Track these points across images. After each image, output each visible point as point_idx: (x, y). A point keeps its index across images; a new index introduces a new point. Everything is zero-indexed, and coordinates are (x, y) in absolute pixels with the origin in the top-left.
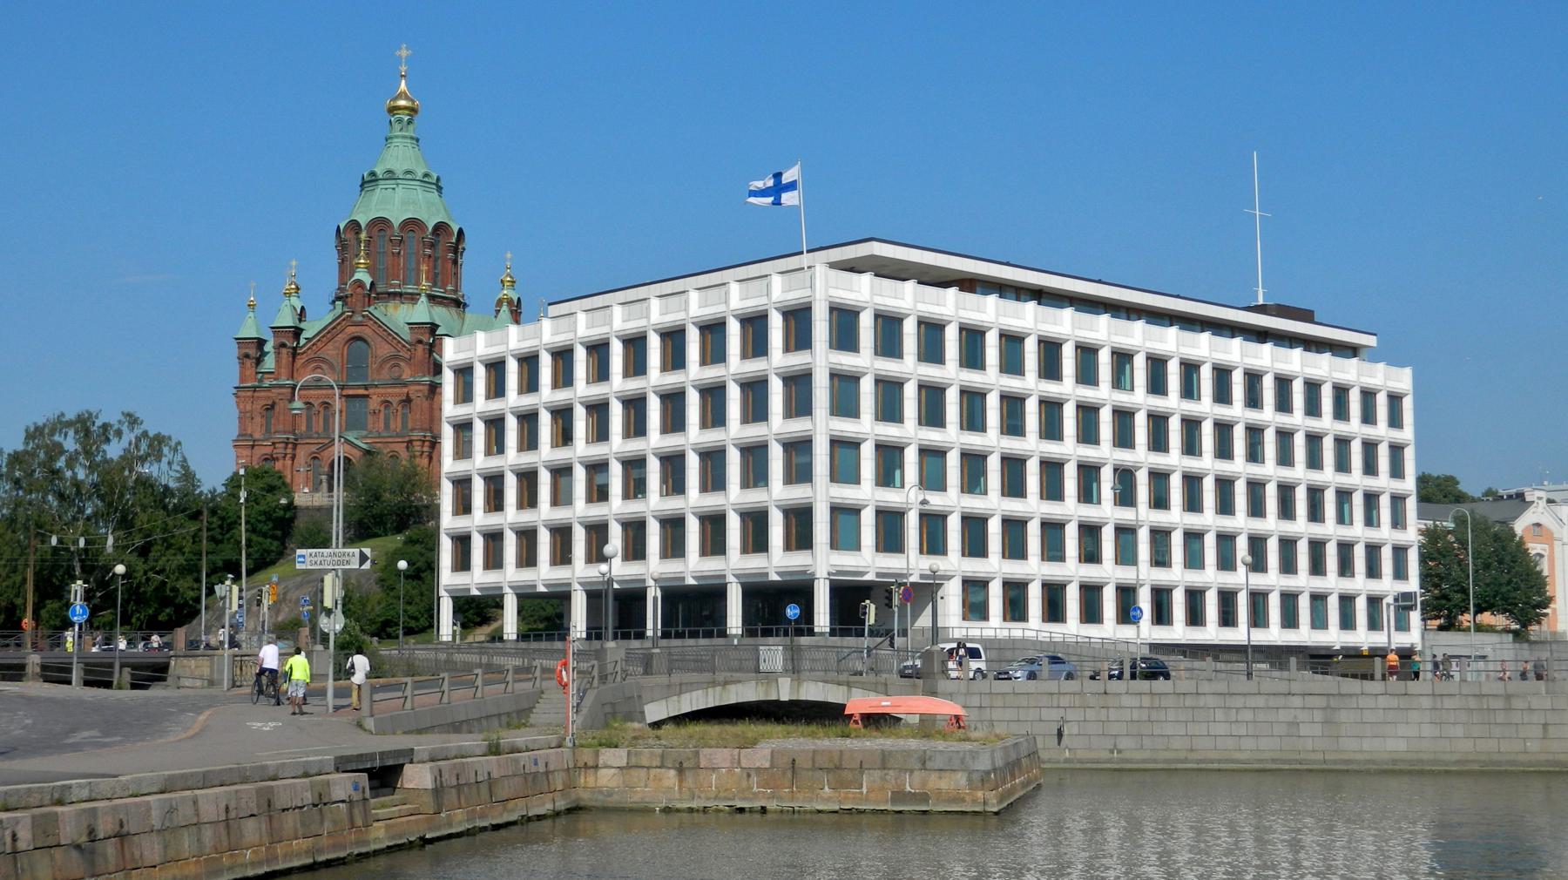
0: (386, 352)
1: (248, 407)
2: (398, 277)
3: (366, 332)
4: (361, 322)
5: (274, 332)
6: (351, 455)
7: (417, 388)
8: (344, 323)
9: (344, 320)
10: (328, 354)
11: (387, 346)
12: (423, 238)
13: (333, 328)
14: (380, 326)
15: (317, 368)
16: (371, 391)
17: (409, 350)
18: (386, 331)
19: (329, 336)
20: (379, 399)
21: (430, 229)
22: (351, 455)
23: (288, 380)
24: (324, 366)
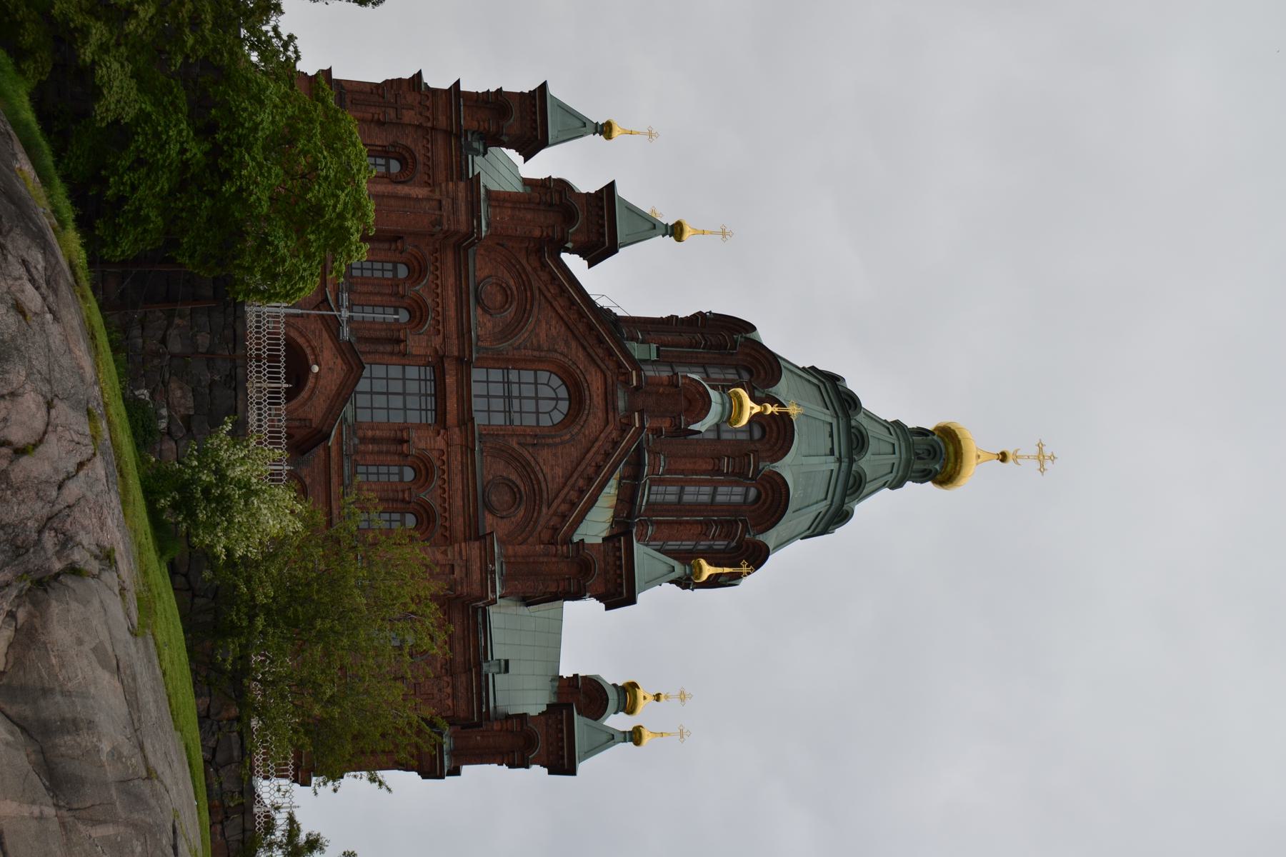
0: (544, 468)
1: (409, 116)
2: (668, 471)
3: (594, 422)
4: (615, 409)
6: (313, 391)
7: (476, 567)
8: (612, 365)
9: (620, 365)
10: (538, 320)
11: (559, 471)
12: (744, 523)
14: (608, 455)
15: (505, 290)
16: (456, 434)
17: (555, 530)
18: (597, 473)
20: (434, 456)
21: (761, 538)
22: (310, 398)
23: (488, 225)
24: (510, 312)
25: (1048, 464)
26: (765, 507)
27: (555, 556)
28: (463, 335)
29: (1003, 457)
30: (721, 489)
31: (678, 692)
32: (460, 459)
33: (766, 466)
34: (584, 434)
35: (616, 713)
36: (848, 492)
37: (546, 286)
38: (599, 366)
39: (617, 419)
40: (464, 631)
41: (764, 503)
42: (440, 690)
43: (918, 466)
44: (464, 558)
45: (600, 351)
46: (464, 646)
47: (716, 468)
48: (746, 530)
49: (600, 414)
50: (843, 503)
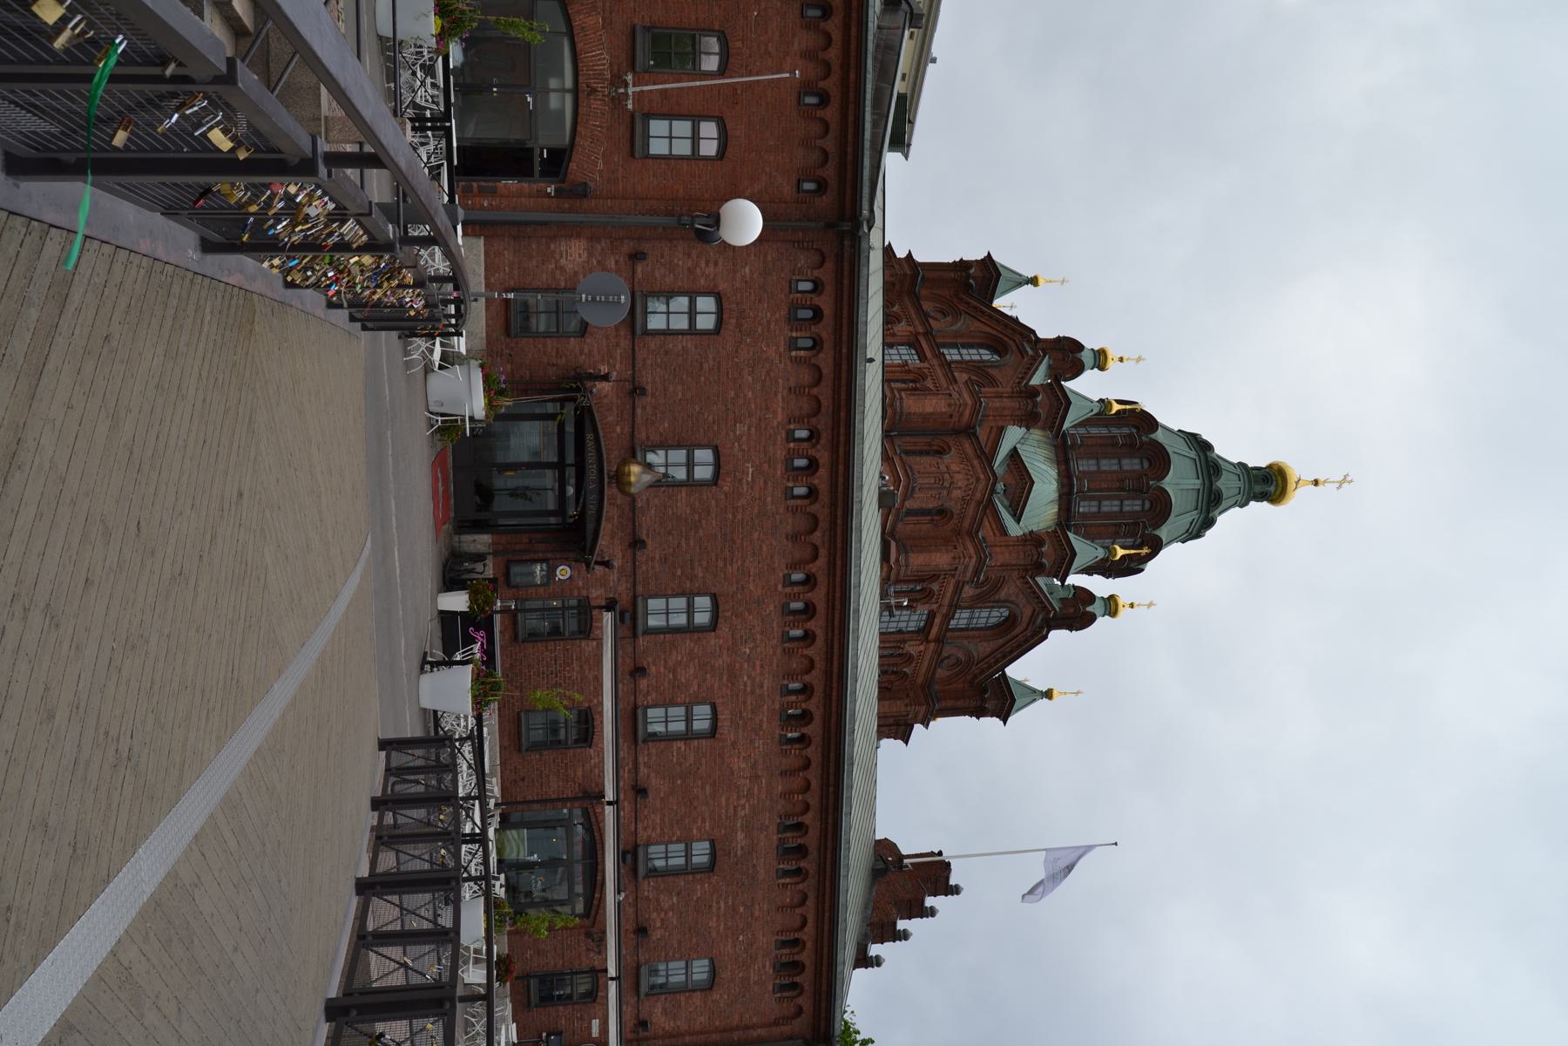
16: (935, 362)
29: (1316, 483)
35: (1103, 616)
43: (1258, 488)
50: (1211, 484)
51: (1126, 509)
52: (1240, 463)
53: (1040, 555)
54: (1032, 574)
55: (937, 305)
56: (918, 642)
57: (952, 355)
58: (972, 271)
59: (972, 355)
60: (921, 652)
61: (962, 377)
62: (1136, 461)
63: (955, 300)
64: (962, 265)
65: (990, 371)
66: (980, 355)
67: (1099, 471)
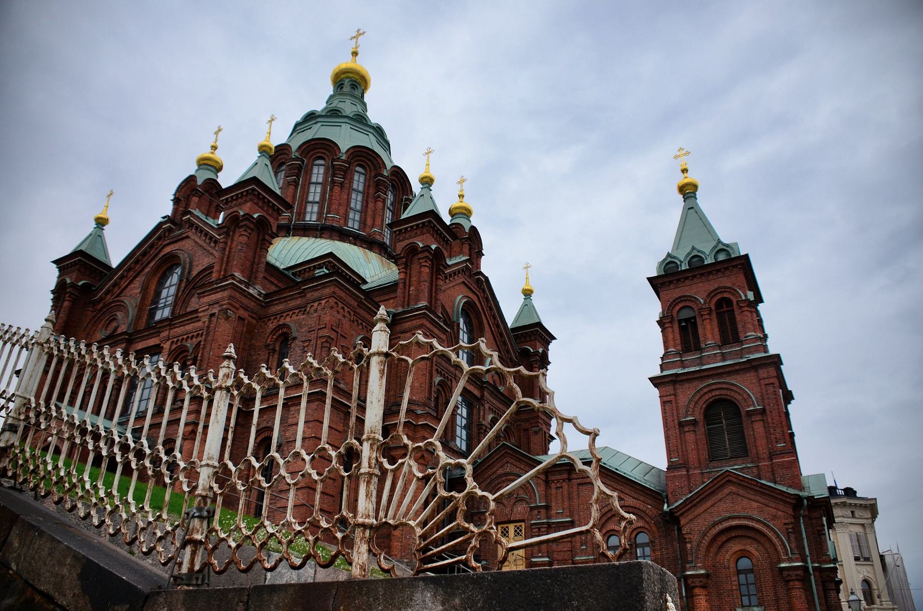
5: (60, 269)
9: (159, 238)
12: (333, 160)
13: (144, 254)
19: (138, 267)
25: (361, 32)
26: (327, 153)
27: (226, 243)
28: (116, 342)
29: (355, 54)
30: (314, 180)
31: (460, 185)
32: (177, 329)
33: (295, 154)
34: (191, 250)
36: (340, 114)
37: (112, 295)
38: (160, 251)
39: (187, 230)
40: (281, 303)
41: (324, 154)
42: (316, 311)
44: (207, 307)
45: (152, 252)
46: (291, 300)
47: (293, 183)
48: (339, 159)
49: (183, 243)
50: (347, 117)
51: (361, 188)
52: (327, 103)
53: (427, 248)
54: (443, 265)
55: (100, 326)
56: (482, 408)
57: (163, 313)
58: (68, 281)
59: (169, 292)
60: (489, 407)
61: (194, 303)
62: (315, 170)
63: (101, 305)
64: (59, 292)
65: (194, 273)
66: (171, 286)
67: (321, 203)
